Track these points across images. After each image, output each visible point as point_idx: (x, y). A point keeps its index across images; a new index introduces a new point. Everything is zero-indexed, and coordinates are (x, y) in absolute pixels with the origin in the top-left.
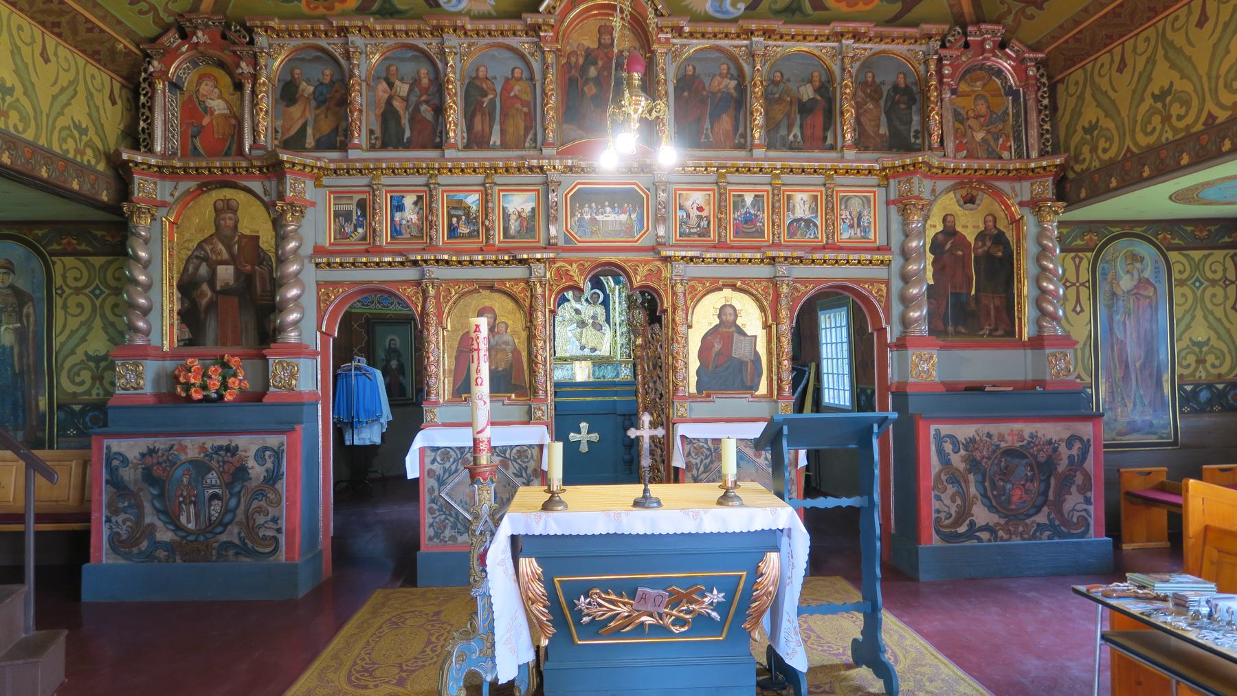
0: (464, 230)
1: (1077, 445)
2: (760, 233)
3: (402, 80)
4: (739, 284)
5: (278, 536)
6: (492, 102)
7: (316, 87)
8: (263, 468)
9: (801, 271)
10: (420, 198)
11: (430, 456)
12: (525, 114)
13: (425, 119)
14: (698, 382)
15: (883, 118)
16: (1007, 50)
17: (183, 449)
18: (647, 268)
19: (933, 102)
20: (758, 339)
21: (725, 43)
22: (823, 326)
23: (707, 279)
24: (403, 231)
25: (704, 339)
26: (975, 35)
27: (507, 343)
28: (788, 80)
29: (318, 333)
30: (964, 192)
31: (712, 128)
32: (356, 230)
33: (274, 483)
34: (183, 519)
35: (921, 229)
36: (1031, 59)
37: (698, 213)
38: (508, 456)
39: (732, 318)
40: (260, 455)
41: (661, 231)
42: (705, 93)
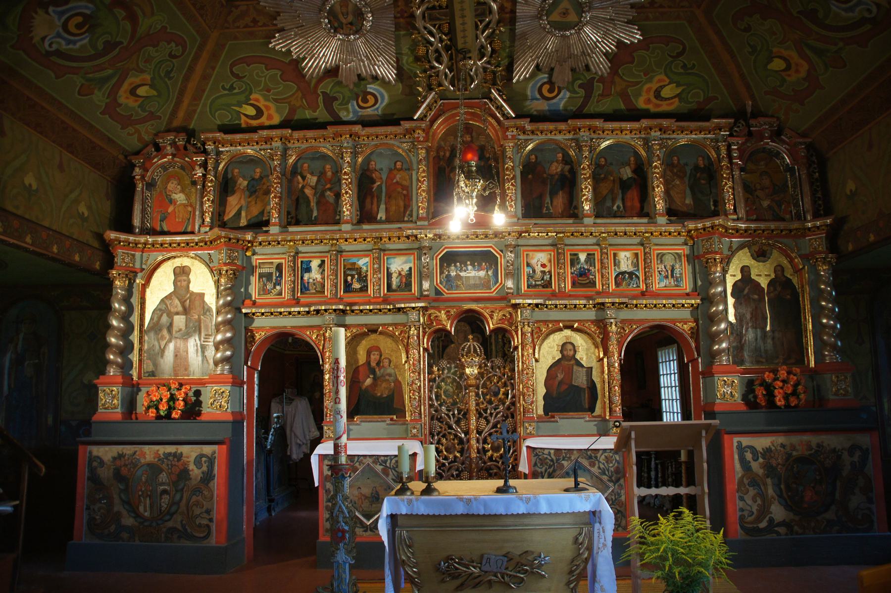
0: (356, 286)
1: (858, 454)
3: (312, 174)
4: (575, 326)
5: (211, 524)
6: (380, 187)
7: (249, 182)
8: (200, 471)
9: (625, 314)
10: (323, 262)
12: (404, 195)
13: (327, 202)
15: (688, 191)
16: (783, 137)
17: (143, 454)
18: (501, 313)
19: (725, 178)
20: (593, 370)
21: (559, 137)
23: (551, 321)
24: (311, 288)
25: (548, 371)
26: (756, 126)
27: (390, 375)
28: (611, 164)
30: (755, 248)
32: (275, 287)
33: (208, 483)
34: (141, 509)
35: (722, 278)
36: (801, 144)
37: (542, 269)
38: (388, 465)
39: (572, 353)
40: (198, 462)
42: (545, 175)
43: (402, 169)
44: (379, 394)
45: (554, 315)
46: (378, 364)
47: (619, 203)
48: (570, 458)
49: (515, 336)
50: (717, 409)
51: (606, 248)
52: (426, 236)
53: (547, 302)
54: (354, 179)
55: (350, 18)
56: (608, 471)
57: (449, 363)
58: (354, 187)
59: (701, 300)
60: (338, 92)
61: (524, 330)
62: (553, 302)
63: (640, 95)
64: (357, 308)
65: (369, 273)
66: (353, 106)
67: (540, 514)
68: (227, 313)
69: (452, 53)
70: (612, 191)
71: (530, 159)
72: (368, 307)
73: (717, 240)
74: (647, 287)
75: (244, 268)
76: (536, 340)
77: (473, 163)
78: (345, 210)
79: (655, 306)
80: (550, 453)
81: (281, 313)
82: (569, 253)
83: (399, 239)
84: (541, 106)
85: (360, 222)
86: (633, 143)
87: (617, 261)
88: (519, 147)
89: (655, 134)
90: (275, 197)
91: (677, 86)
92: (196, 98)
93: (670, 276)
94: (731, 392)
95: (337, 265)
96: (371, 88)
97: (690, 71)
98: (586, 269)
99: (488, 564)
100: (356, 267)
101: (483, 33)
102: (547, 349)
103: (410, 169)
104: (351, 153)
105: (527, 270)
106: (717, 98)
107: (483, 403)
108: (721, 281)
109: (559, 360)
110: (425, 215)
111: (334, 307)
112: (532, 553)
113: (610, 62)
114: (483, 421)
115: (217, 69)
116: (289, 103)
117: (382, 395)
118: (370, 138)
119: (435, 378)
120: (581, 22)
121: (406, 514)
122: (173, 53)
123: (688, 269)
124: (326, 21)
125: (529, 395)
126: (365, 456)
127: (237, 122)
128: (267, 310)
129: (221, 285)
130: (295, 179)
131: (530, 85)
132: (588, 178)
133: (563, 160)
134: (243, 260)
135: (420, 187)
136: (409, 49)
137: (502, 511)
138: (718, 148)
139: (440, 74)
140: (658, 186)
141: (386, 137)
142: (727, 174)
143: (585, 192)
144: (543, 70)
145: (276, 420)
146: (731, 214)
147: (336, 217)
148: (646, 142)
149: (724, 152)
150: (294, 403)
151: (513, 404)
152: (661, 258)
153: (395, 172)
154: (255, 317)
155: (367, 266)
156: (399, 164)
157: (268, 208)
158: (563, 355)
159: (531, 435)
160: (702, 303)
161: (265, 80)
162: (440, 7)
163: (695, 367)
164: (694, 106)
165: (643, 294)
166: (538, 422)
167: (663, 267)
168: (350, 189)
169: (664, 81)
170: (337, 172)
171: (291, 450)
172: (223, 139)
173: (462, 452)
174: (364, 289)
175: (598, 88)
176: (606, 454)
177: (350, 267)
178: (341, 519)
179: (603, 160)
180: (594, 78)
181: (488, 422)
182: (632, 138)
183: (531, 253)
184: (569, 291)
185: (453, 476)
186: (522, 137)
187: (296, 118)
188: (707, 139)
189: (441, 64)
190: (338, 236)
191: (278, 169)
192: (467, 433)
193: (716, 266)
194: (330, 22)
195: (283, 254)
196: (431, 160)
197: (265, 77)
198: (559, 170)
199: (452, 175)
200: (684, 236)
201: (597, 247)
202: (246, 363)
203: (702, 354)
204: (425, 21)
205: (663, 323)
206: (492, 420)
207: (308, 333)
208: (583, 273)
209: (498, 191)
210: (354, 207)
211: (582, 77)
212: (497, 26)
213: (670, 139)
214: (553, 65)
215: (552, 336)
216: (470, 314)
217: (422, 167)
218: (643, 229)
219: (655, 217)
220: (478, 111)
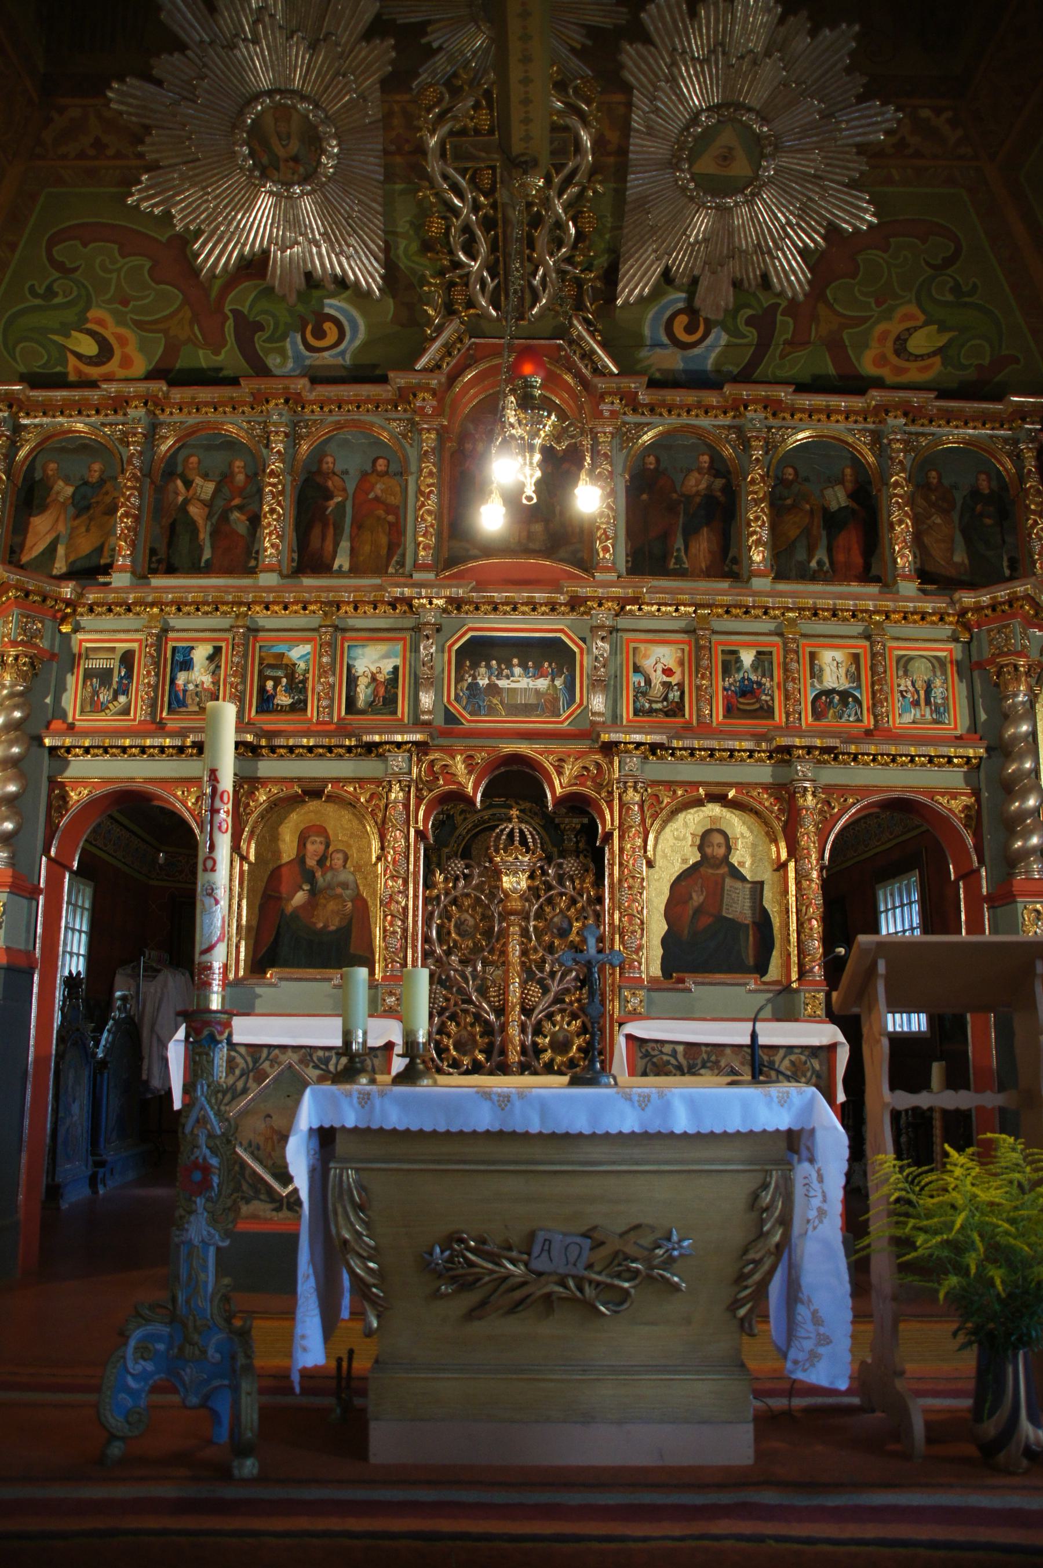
0: (284, 699)
2: (769, 712)
3: (205, 476)
4: (731, 794)
6: (341, 506)
7: (77, 488)
9: (833, 775)
10: (218, 650)
14: (663, 958)
15: (959, 537)
18: (580, 764)
19: (1034, 512)
20: (766, 887)
21: (705, 422)
22: (882, 909)
23: (682, 784)
24: (189, 701)
25: (674, 886)
27: (345, 885)
28: (807, 480)
29: (44, 859)
32: (115, 698)
35: (1028, 706)
37: (666, 679)
38: (332, 1068)
39: (722, 851)
41: (598, 703)
43: (386, 473)
44: (321, 925)
46: (321, 862)
47: (821, 554)
52: (431, 603)
53: (675, 744)
54: (288, 488)
55: (294, 146)
57: (467, 867)
58: (288, 501)
59: (988, 750)
62: (687, 743)
63: (867, 346)
65: (310, 676)
66: (294, 344)
67: (672, 1134)
69: (496, 236)
71: (644, 464)
72: (305, 741)
74: (876, 721)
75: (53, 656)
76: (648, 821)
78: (267, 544)
80: (675, 1052)
81: (124, 749)
83: (375, 608)
84: (672, 360)
86: (850, 440)
87: (817, 668)
90: (126, 515)
95: (245, 656)
96: (331, 306)
97: (967, 299)
98: (753, 682)
99: (545, 1254)
100: (285, 661)
101: (560, 195)
102: (672, 841)
103: (402, 473)
106: (1017, 361)
107: (535, 950)
108: (1026, 712)
109: (696, 865)
112: (653, 1229)
114: (535, 989)
116: (165, 332)
117: (325, 926)
118: (326, 409)
119: (438, 897)
120: (757, 177)
121: (356, 1130)
123: (962, 688)
124: (245, 150)
127: (58, 369)
128: (97, 742)
130: (171, 487)
131: (650, 315)
134: (53, 639)
135: (423, 505)
136: (412, 223)
137: (581, 1124)
138: (1018, 456)
139: (472, 279)
140: (901, 522)
141: (358, 407)
142: (1037, 504)
143: (754, 527)
145: (119, 1003)
147: (248, 562)
148: (877, 437)
150: (161, 977)
153: (373, 479)
154: (70, 757)
155: (307, 661)
158: (704, 856)
159: (635, 1016)
160: (989, 757)
161: (119, 276)
162: (477, 132)
165: (869, 733)
166: (649, 990)
167: (909, 683)
168: (279, 504)
170: (256, 474)
171: (149, 1069)
172: (28, 397)
173: (488, 1051)
174: (299, 707)
175: (785, 327)
176: (793, 1057)
177: (272, 661)
178: (202, 1140)
179: (790, 470)
181: (546, 990)
182: (850, 430)
183: (642, 647)
184: (718, 723)
186: (631, 418)
187: (178, 366)
188: (997, 437)
189: (475, 260)
191: (136, 462)
192: (501, 1011)
194: (252, 155)
195: (137, 631)
197: (119, 270)
198: (703, 486)
200: (951, 623)
201: (776, 639)
202: (46, 851)
203: (987, 859)
205: (907, 795)
206: (554, 988)
207: (179, 793)
209: (587, 442)
210: (287, 540)
212: (589, 181)
213: (923, 434)
214: (696, 272)
215: (681, 816)
216: (515, 768)
217: (428, 466)
218: (870, 605)
219: (895, 583)
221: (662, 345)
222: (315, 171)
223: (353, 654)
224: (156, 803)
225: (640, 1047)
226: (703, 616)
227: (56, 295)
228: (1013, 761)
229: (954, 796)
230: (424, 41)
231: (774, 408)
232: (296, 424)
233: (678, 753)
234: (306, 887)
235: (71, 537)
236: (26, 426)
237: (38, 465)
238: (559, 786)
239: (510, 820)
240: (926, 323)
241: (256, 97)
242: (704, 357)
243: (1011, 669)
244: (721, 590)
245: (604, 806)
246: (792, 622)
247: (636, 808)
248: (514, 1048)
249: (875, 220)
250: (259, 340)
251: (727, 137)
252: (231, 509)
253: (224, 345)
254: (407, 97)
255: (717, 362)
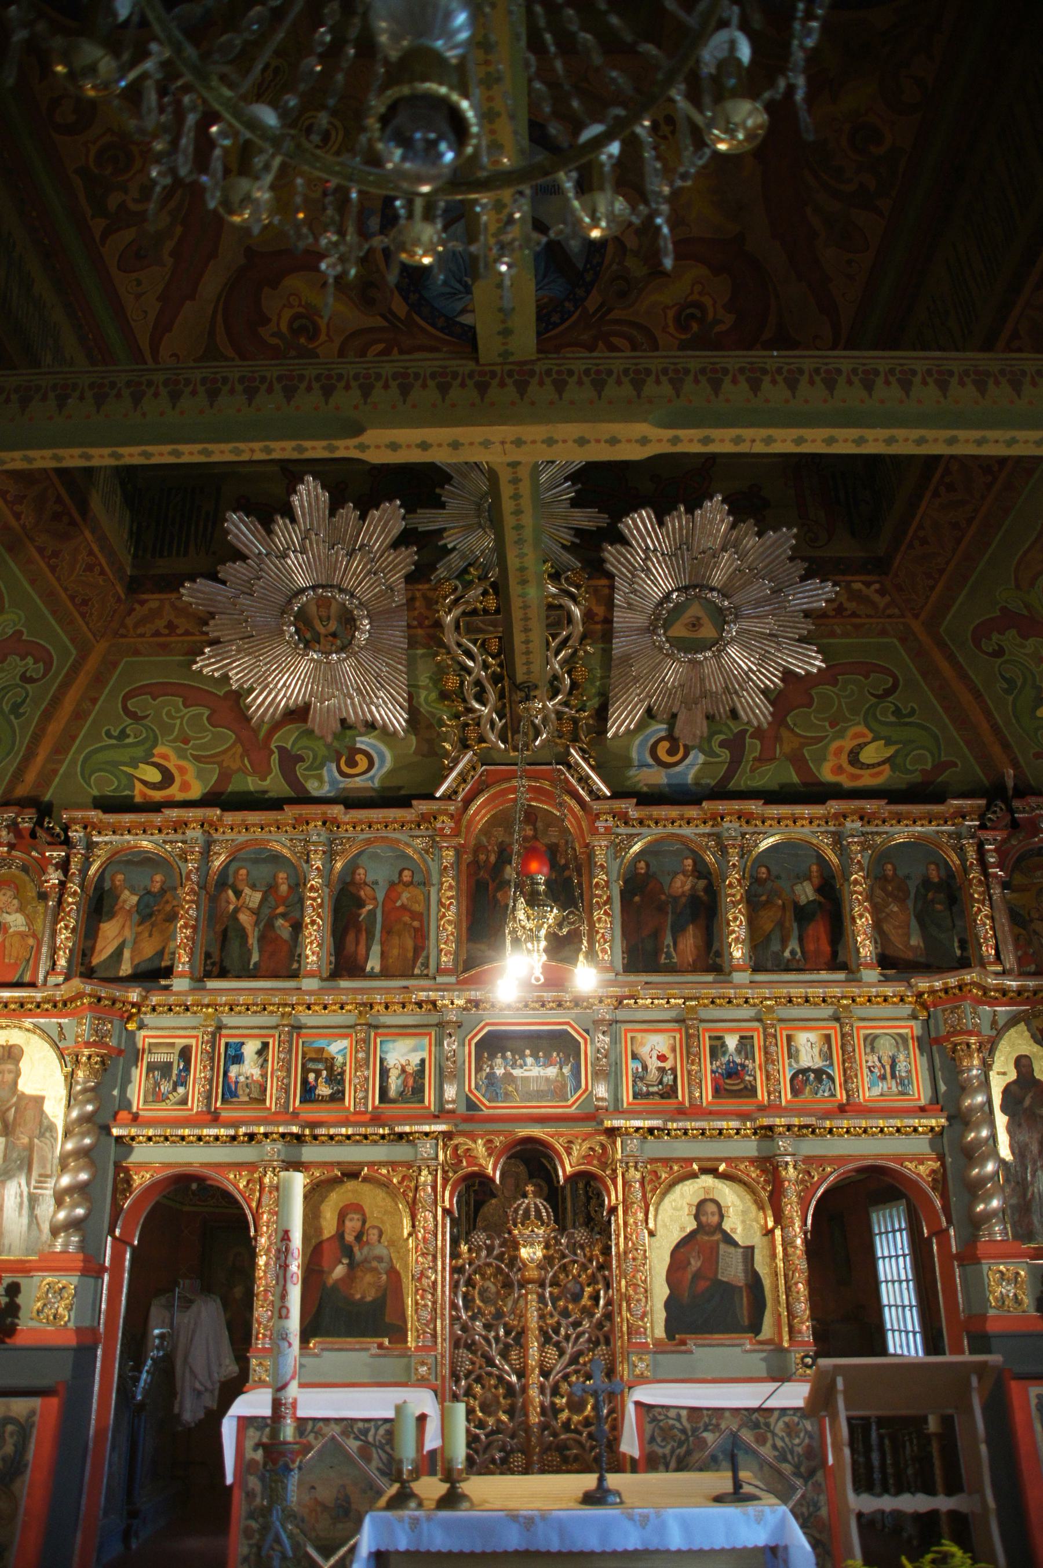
2: (752, 1091)
3: (253, 887)
4: (722, 1167)
6: (372, 913)
9: (812, 1147)
10: (265, 1045)
11: (253, 1436)
12: (416, 930)
13: (278, 937)
15: (914, 923)
18: (586, 1145)
19: (978, 901)
20: (756, 1251)
21: (687, 831)
22: (877, 1231)
23: (677, 1160)
24: (240, 1092)
25: (674, 1253)
26: (1024, 812)
27: (380, 1259)
28: (778, 877)
31: (675, 944)
32: (175, 1089)
35: (982, 1078)
38: (370, 1439)
39: (715, 1219)
42: (663, 897)
43: (411, 883)
44: (358, 1296)
45: (683, 1149)
46: (359, 1237)
47: (793, 945)
48: (718, 1425)
49: (612, 1188)
50: (991, 1328)
51: (773, 1026)
53: (670, 1125)
54: (326, 899)
55: (333, 626)
56: (792, 1452)
57: (489, 1237)
58: (327, 912)
59: (948, 1119)
60: (306, 748)
61: (628, 1176)
62: (681, 1125)
63: (825, 759)
64: (322, 1131)
65: (347, 1068)
66: (330, 771)
68: (84, 1135)
69: (503, 688)
70: (781, 924)
71: (636, 868)
72: (343, 1131)
73: (969, 1010)
74: (848, 1096)
75: (120, 1052)
76: (649, 1195)
77: (541, 878)
78: (308, 952)
79: (865, 1131)
81: (183, 1138)
82: (707, 1035)
83: (404, 1007)
84: (655, 777)
85: (335, 974)
86: (815, 841)
87: (793, 1049)
88: (618, 848)
89: (853, 825)
91: (886, 745)
92: (60, 750)
93: (888, 1076)
94: (1015, 1295)
95: (290, 1051)
96: (362, 742)
97: (907, 720)
100: (325, 1055)
101: (557, 654)
102: (670, 1212)
103: (425, 883)
104: (324, 852)
105: (632, 1065)
106: (955, 765)
107: (552, 1316)
108: (981, 1084)
109: (693, 1233)
110: (450, 965)
111: (281, 1130)
113: (772, 703)
114: (552, 1351)
115: (100, 702)
116: (220, 764)
117: (363, 1298)
118: (358, 829)
119: (463, 1266)
120: (721, 638)
122: (28, 674)
124: (293, 629)
125: (639, 1300)
126: (326, 1420)
128: (159, 1132)
129: (77, 1083)
130: (223, 895)
131: (637, 742)
132: (739, 902)
133: (694, 870)
134: (120, 1037)
135: (444, 916)
136: (431, 678)
138: (961, 849)
139: (483, 722)
140: (861, 916)
142: (979, 894)
144: (659, 718)
145: (157, 1341)
146: (991, 963)
148: (838, 838)
149: (972, 855)
150: (194, 1308)
151: (608, 1316)
152: (872, 1043)
154: (134, 1144)
155: (344, 1056)
156: (407, 876)
157: (172, 945)
159: (642, 1380)
160: (950, 1125)
162: (486, 611)
163: (944, 1245)
164: (916, 778)
166: (655, 1353)
168: (319, 916)
169: (864, 735)
170: (298, 885)
172: (101, 821)
173: (511, 1412)
174: (338, 1097)
175: (753, 748)
176: (786, 1419)
177: (314, 1056)
179: (763, 870)
180: (745, 731)
181: (562, 1353)
183: (639, 1035)
184: (708, 1103)
185: (493, 1461)
186: (622, 830)
187: (230, 789)
188: (942, 832)
189: (485, 705)
190: (294, 1000)
191: (194, 877)
192: (521, 1374)
193: (971, 1056)
194: (297, 632)
195: (194, 1028)
196: (464, 867)
197: (182, 718)
198: (687, 887)
199: (499, 895)
200: (910, 1003)
201: (756, 1024)
202: (111, 1232)
204: (459, 634)
206: (570, 1349)
207: (232, 1176)
208: (733, 1072)
209: (584, 928)
210: (325, 947)
211: (724, 729)
212: (581, 644)
213: (878, 833)
214: (675, 710)
215: (678, 1188)
216: (529, 1146)
217: (449, 881)
218: (837, 991)
219: (859, 970)
220: (546, 785)
221: (649, 766)
222: (350, 643)
223: (385, 1048)
224: (209, 1182)
225: (648, 1411)
226: (693, 1007)
227: (128, 736)
228: (971, 1131)
229: (921, 1162)
230: (441, 543)
231: (746, 818)
232: (332, 842)
233: (673, 1133)
234: (345, 1261)
235: (135, 942)
236: (97, 843)
237: (107, 876)
238: (567, 1167)
239: (525, 1195)
240: (874, 740)
241: (303, 591)
242: (685, 774)
243: (964, 1047)
244: (704, 984)
245: (609, 1182)
246: (770, 1008)
247: (637, 1185)
248: (535, 1408)
249: (823, 665)
250: (300, 769)
251: (695, 610)
252: (276, 917)
253: (270, 772)
254: (426, 586)
255: (697, 777)
